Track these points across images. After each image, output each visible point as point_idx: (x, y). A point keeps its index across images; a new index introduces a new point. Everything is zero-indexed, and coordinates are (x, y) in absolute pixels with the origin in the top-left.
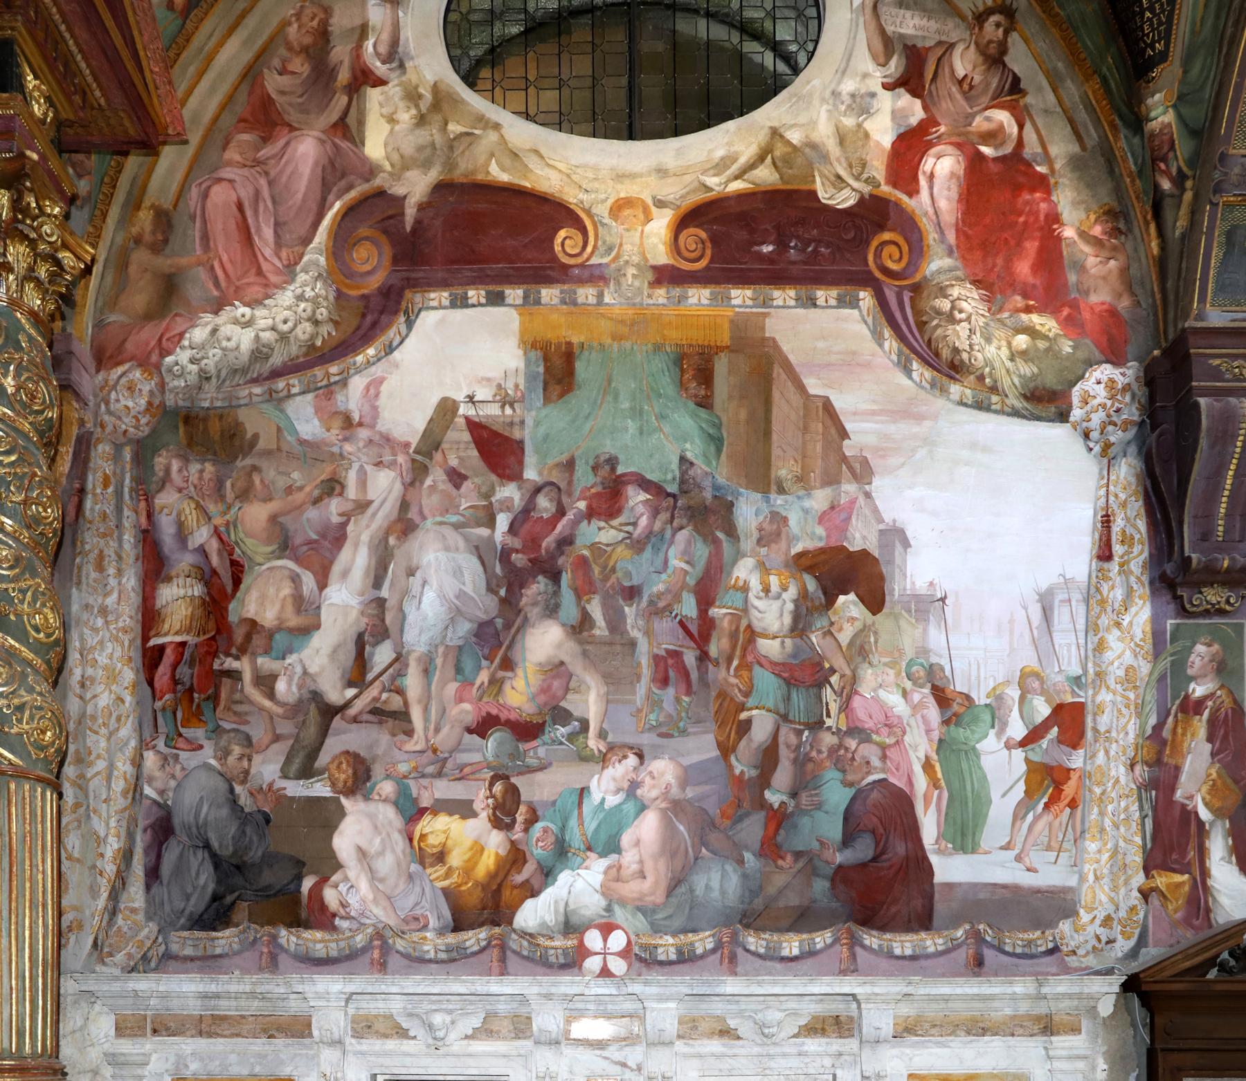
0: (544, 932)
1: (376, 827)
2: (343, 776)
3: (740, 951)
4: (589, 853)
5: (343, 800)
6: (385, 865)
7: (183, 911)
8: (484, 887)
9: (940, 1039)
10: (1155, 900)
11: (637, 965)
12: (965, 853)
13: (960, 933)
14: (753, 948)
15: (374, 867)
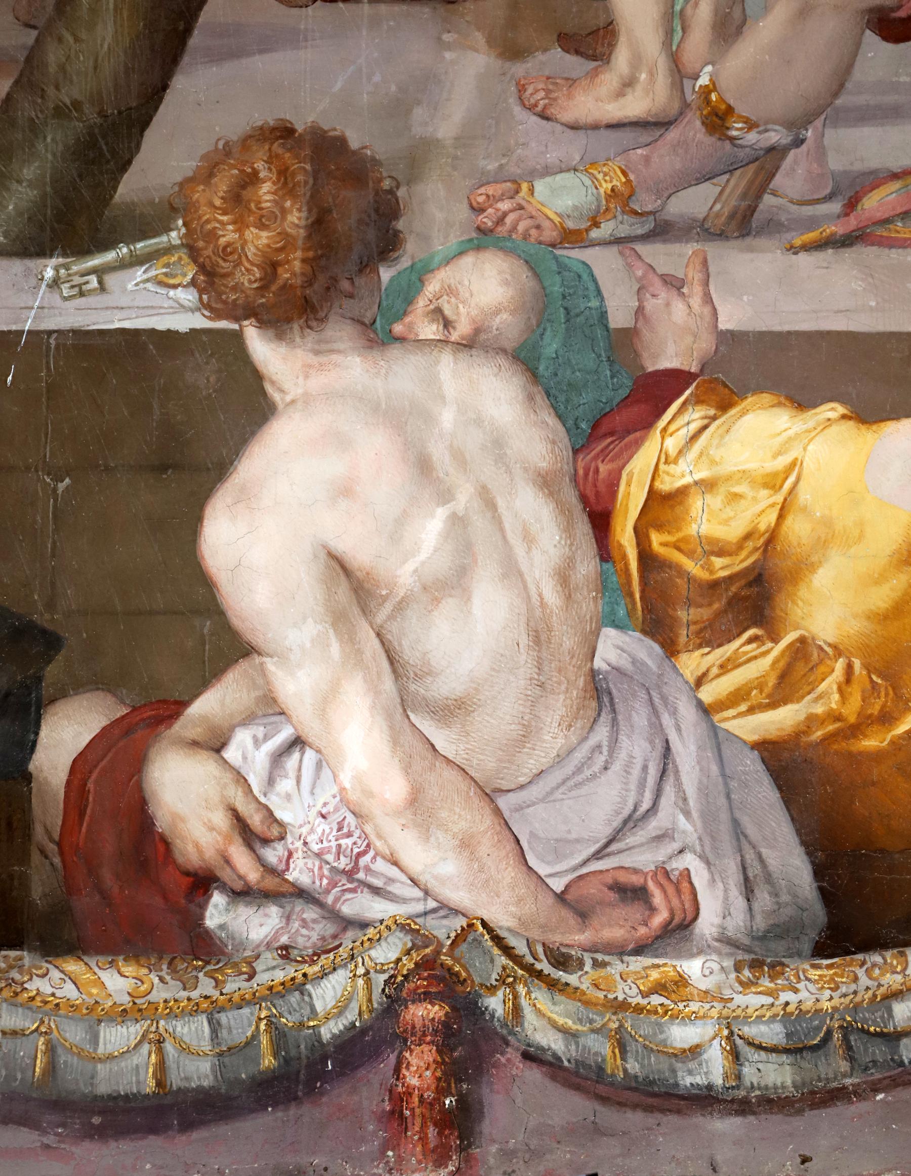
1: (424, 466)
2: (258, 240)
5: (260, 347)
6: (472, 639)
15: (409, 653)
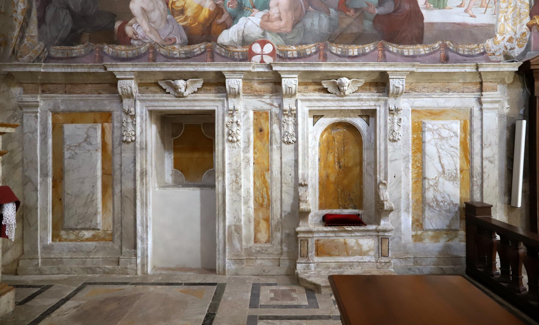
0: (233, 45)
3: (328, 53)
4: (254, 9)
6: (155, 16)
7: (57, 37)
8: (203, 24)
9: (427, 94)
10: (535, 29)
11: (277, 59)
12: (439, 9)
13: (437, 45)
14: (334, 52)
15: (150, 17)
